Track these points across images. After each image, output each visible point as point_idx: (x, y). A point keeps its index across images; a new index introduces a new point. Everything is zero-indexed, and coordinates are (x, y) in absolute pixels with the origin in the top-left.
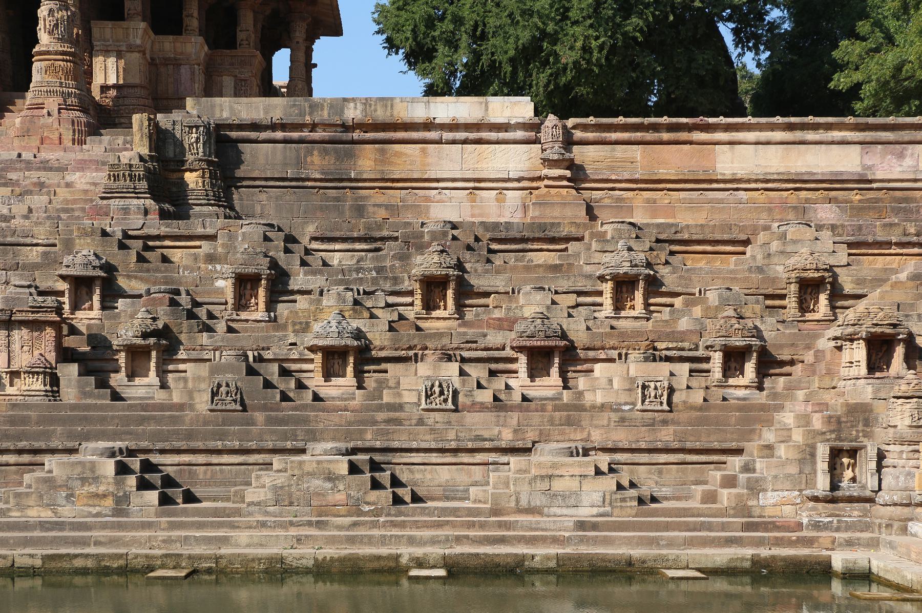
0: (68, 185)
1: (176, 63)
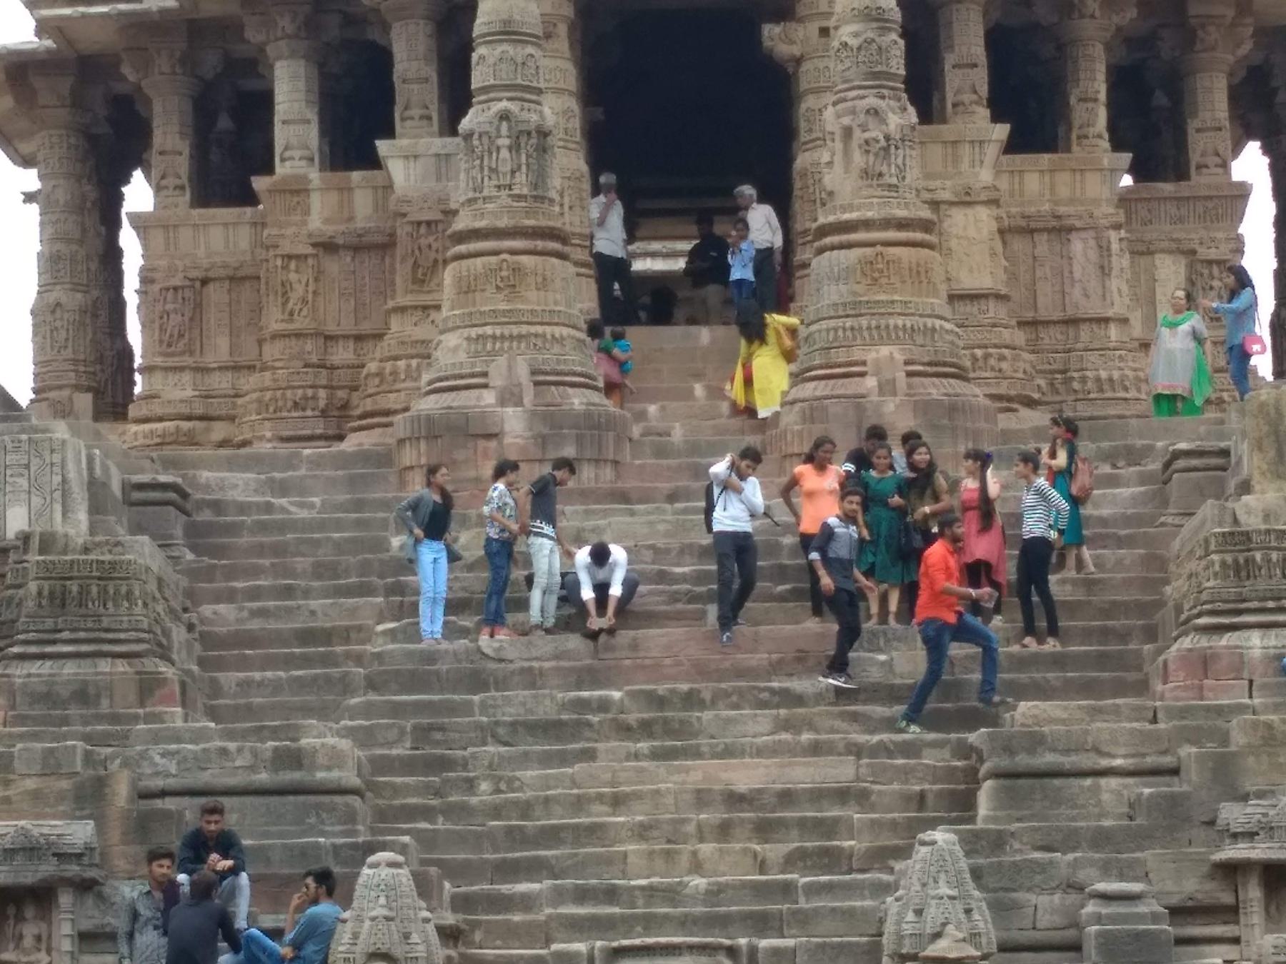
1: (1061, 230)
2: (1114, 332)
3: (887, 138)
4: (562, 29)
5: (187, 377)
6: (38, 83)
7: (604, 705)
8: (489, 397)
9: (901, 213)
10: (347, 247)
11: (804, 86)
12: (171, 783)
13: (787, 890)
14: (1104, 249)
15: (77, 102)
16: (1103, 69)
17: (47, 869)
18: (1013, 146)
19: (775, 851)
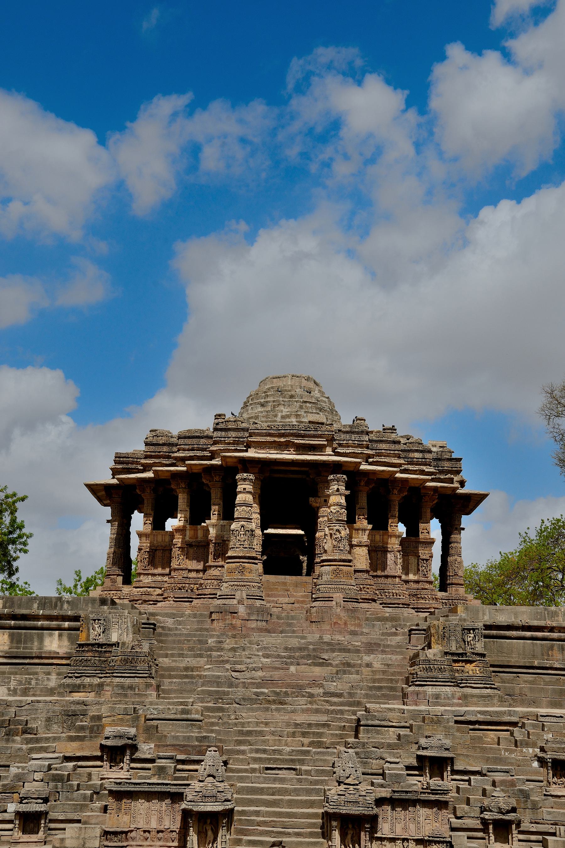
0: (368, 665)
2: (397, 579)
3: (341, 537)
7: (263, 693)
8: (235, 602)
9: (344, 558)
10: (195, 546)
18: (372, 529)
19: (306, 741)
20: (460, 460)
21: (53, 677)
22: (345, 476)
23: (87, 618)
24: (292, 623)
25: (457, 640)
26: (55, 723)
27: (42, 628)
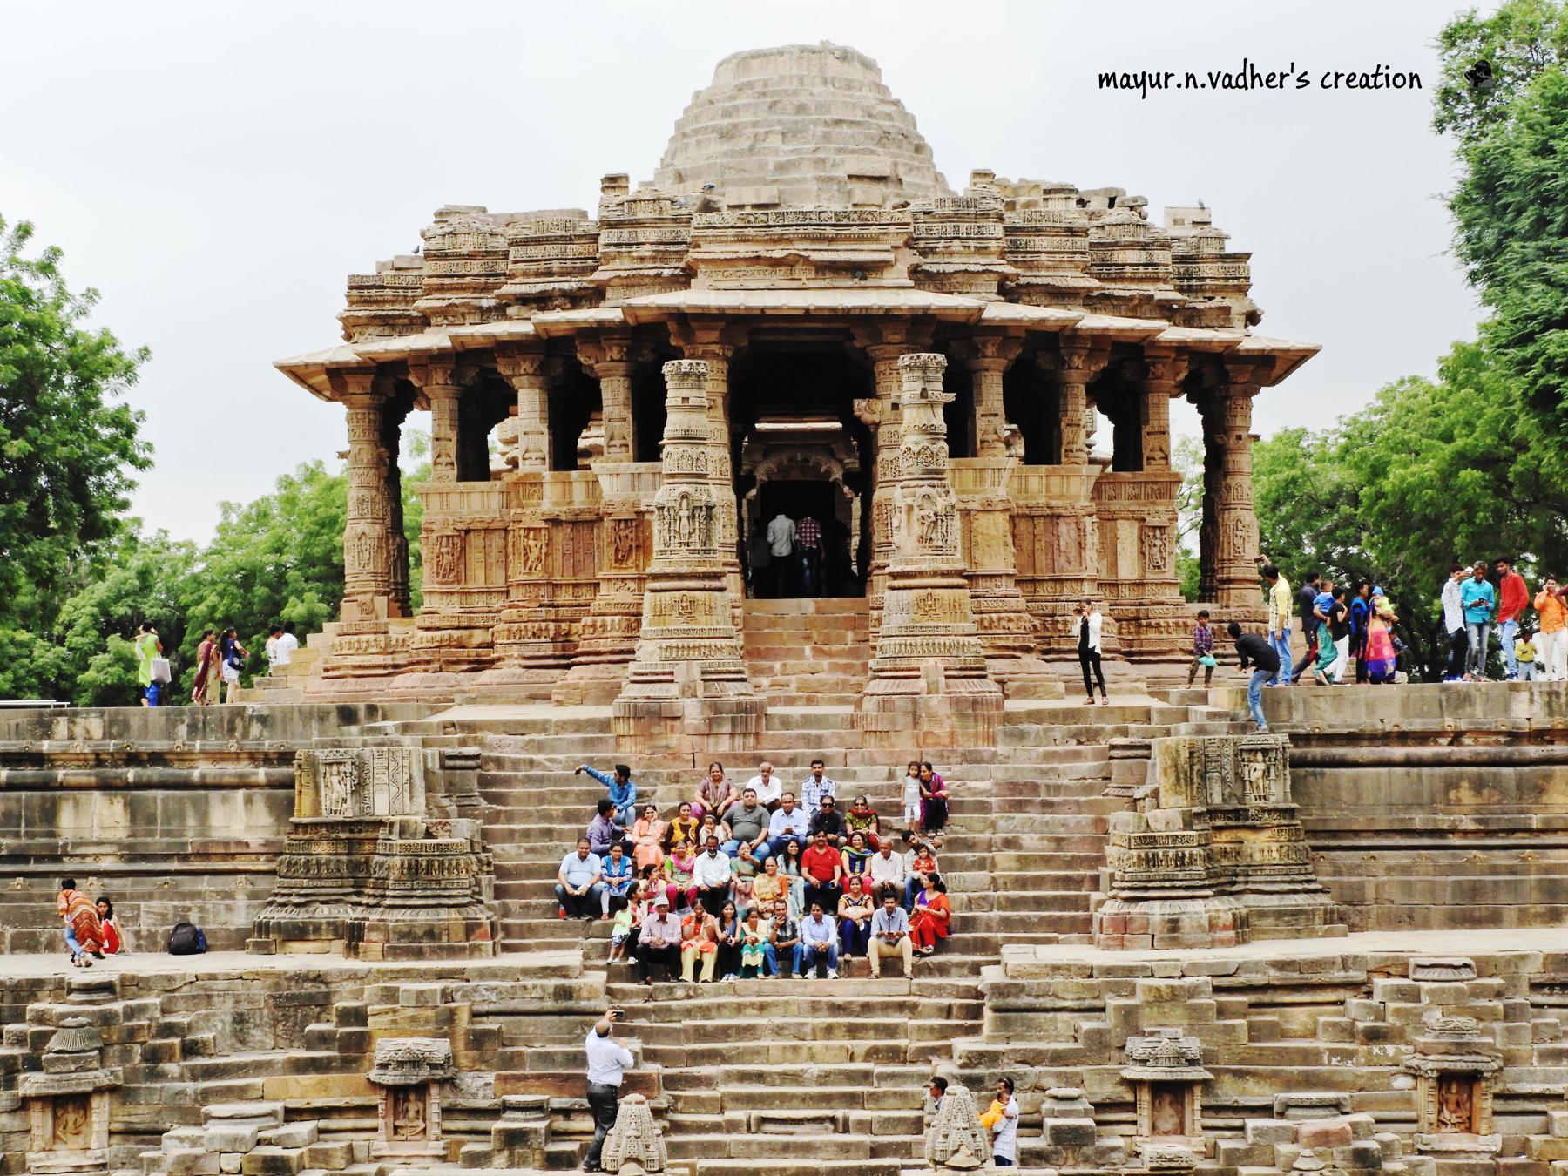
0: (1009, 844)
1: (1054, 518)
3: (936, 515)
4: (720, 401)
5: (456, 598)
6: (349, 379)
8: (674, 690)
9: (945, 567)
10: (567, 522)
11: (880, 443)
12: (492, 1007)
13: (866, 1076)
14: (1081, 530)
15: (375, 390)
16: (1082, 387)
17: (424, 1073)
20: (1248, 256)
21: (241, 901)
22: (941, 357)
23: (313, 764)
24: (819, 738)
25: (1223, 780)
26: (256, 1026)
27: (205, 786)
